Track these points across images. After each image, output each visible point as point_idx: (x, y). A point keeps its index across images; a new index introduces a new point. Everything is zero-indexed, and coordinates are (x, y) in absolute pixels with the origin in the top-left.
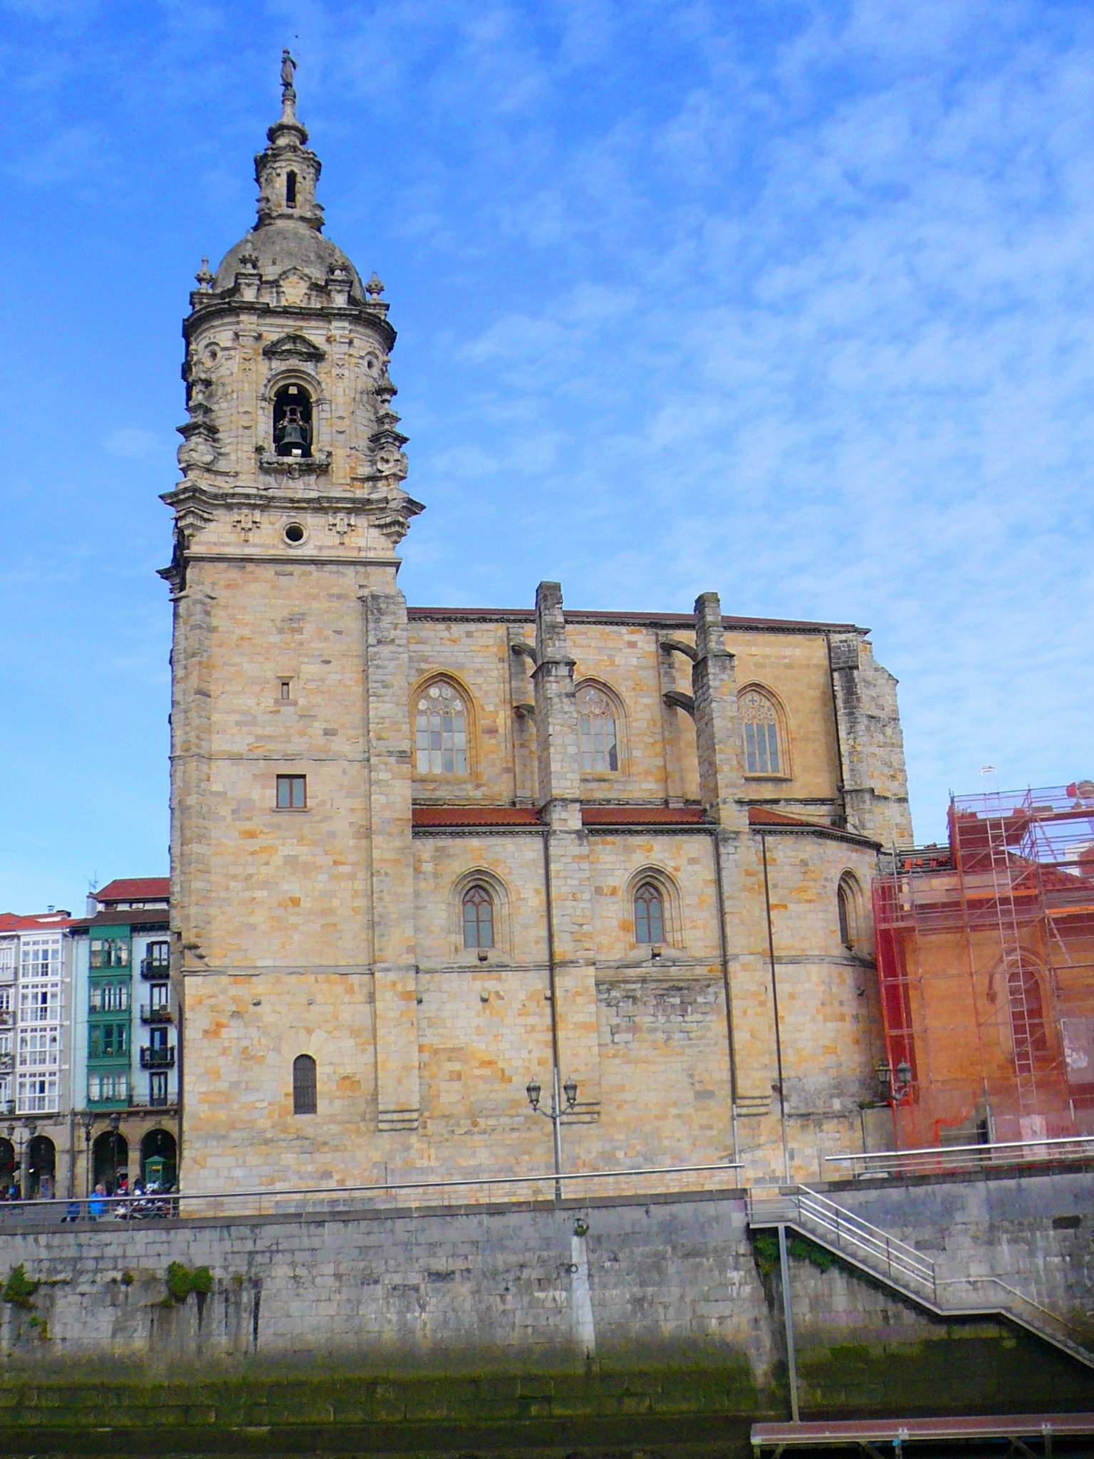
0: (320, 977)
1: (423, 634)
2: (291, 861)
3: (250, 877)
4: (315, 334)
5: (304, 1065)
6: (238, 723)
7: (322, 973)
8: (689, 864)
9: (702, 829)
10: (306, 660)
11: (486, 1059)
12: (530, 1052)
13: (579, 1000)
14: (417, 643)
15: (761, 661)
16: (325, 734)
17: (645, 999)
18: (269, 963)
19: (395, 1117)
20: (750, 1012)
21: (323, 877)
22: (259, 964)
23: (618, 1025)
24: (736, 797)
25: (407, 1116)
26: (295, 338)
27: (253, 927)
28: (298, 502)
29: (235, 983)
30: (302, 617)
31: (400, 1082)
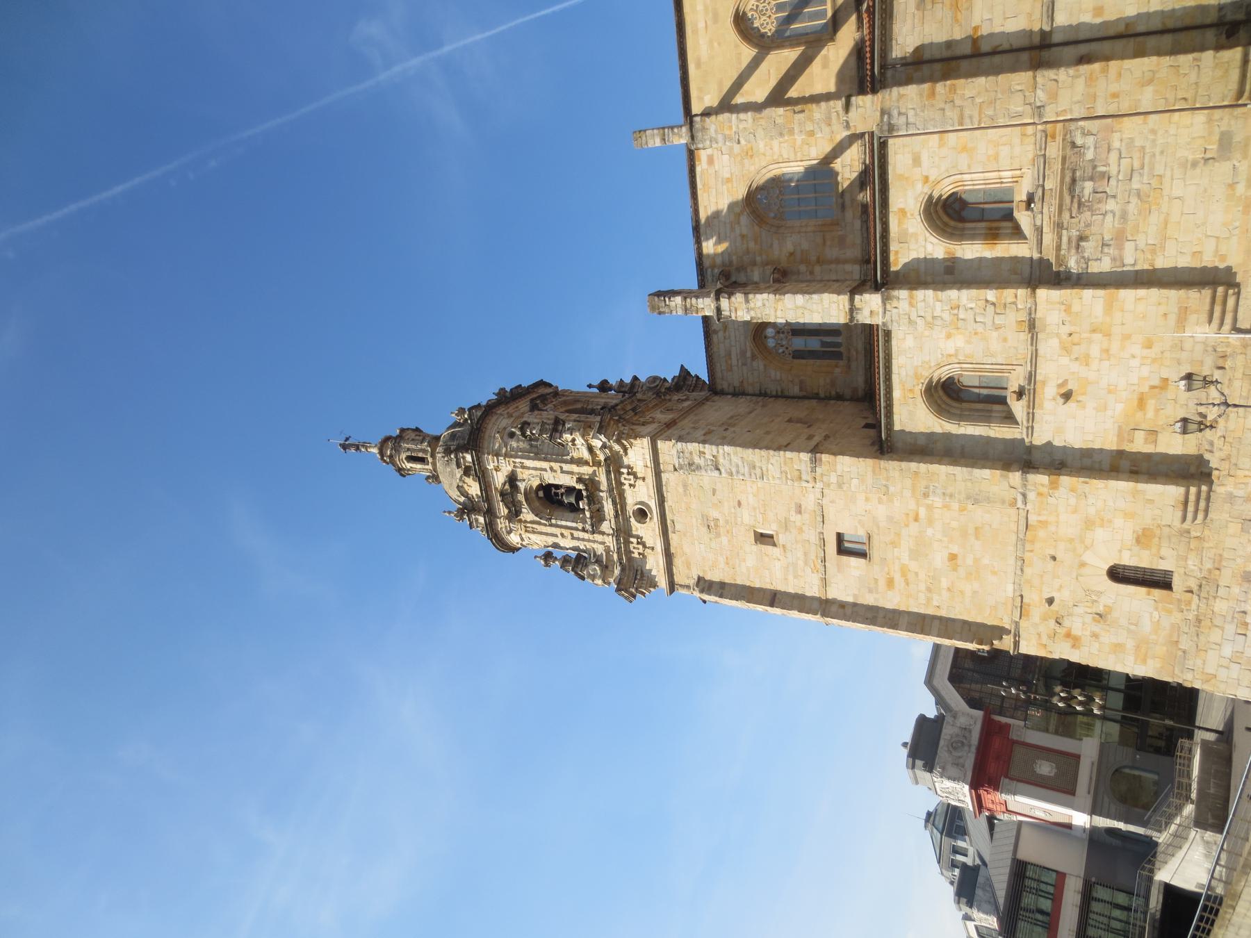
0: (1028, 547)
1: (722, 353)
2: (915, 554)
3: (929, 590)
4: (499, 479)
5: (1118, 575)
6: (796, 577)
7: (1024, 549)
8: (920, 166)
9: (880, 152)
10: (739, 519)
11: (1135, 403)
12: (1134, 357)
13: (1076, 307)
14: (731, 358)
15: (711, 15)
16: (800, 512)
17: (1082, 224)
18: (1010, 588)
19: (1191, 508)
20: (1114, 87)
21: (930, 532)
22: (1011, 595)
23: (1114, 259)
24: (841, 112)
25: (1192, 498)
26: (503, 494)
27: (975, 592)
28: (617, 512)
29: (1028, 615)
30: (705, 517)
31: (1151, 501)
